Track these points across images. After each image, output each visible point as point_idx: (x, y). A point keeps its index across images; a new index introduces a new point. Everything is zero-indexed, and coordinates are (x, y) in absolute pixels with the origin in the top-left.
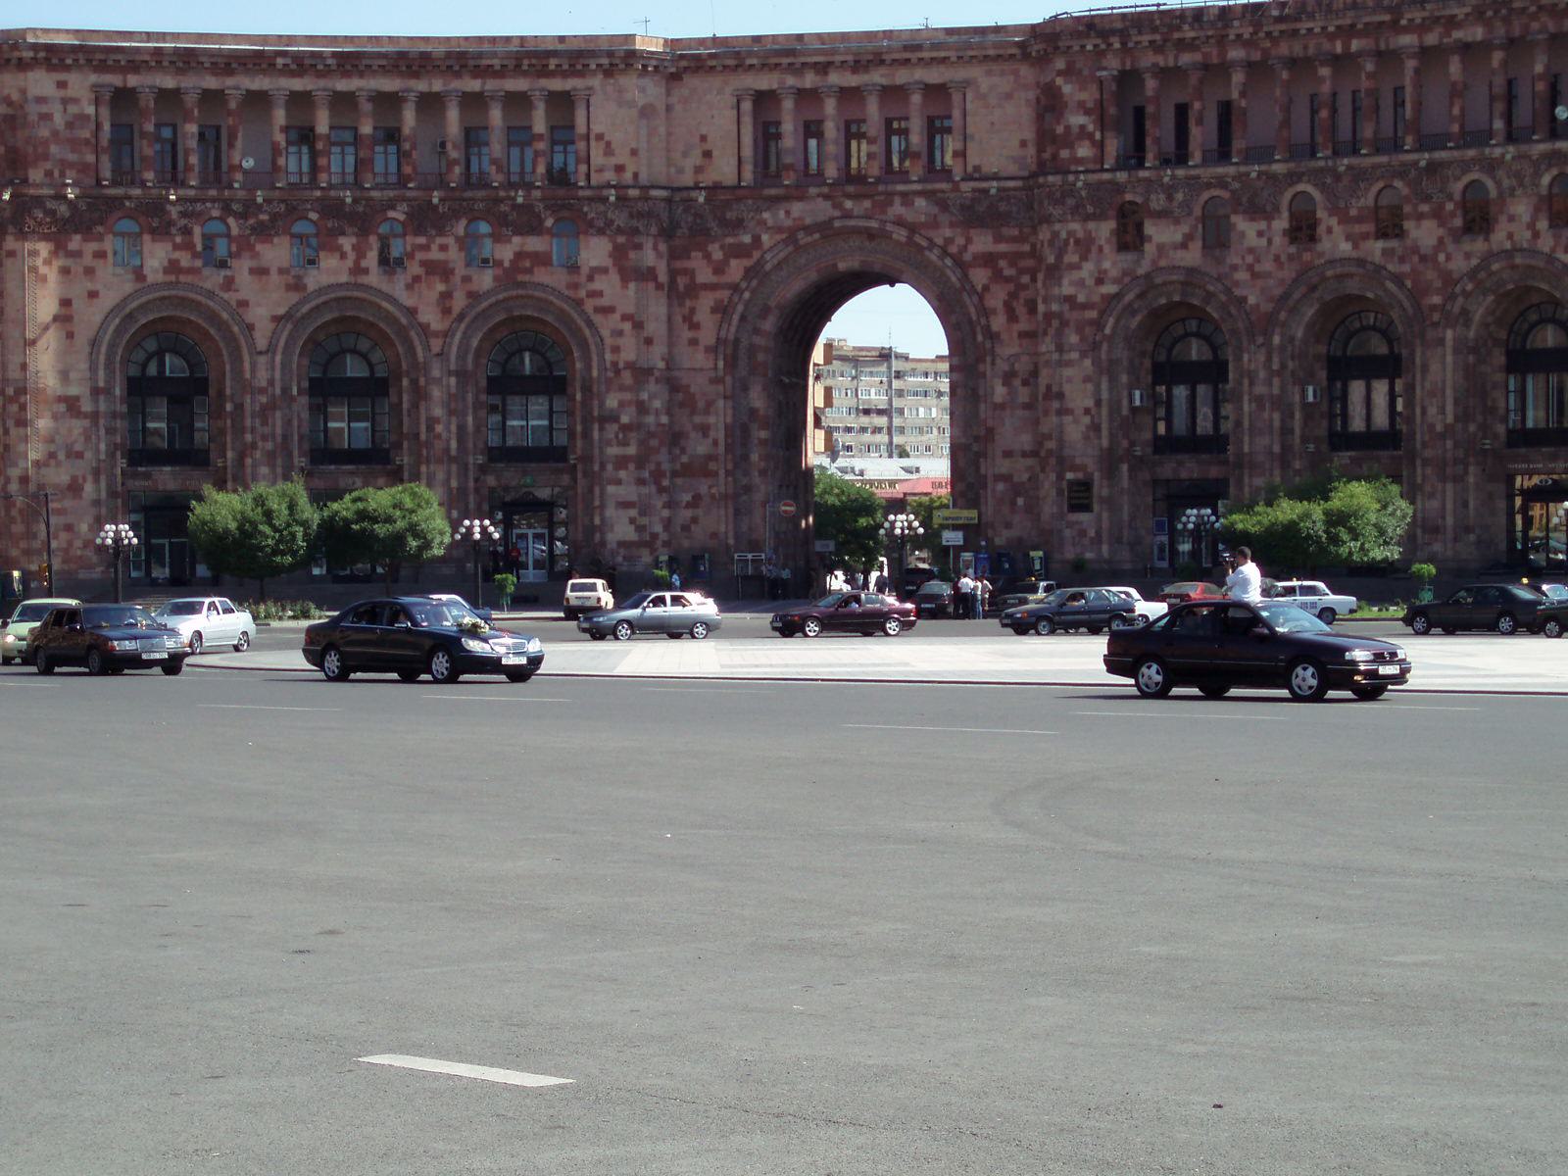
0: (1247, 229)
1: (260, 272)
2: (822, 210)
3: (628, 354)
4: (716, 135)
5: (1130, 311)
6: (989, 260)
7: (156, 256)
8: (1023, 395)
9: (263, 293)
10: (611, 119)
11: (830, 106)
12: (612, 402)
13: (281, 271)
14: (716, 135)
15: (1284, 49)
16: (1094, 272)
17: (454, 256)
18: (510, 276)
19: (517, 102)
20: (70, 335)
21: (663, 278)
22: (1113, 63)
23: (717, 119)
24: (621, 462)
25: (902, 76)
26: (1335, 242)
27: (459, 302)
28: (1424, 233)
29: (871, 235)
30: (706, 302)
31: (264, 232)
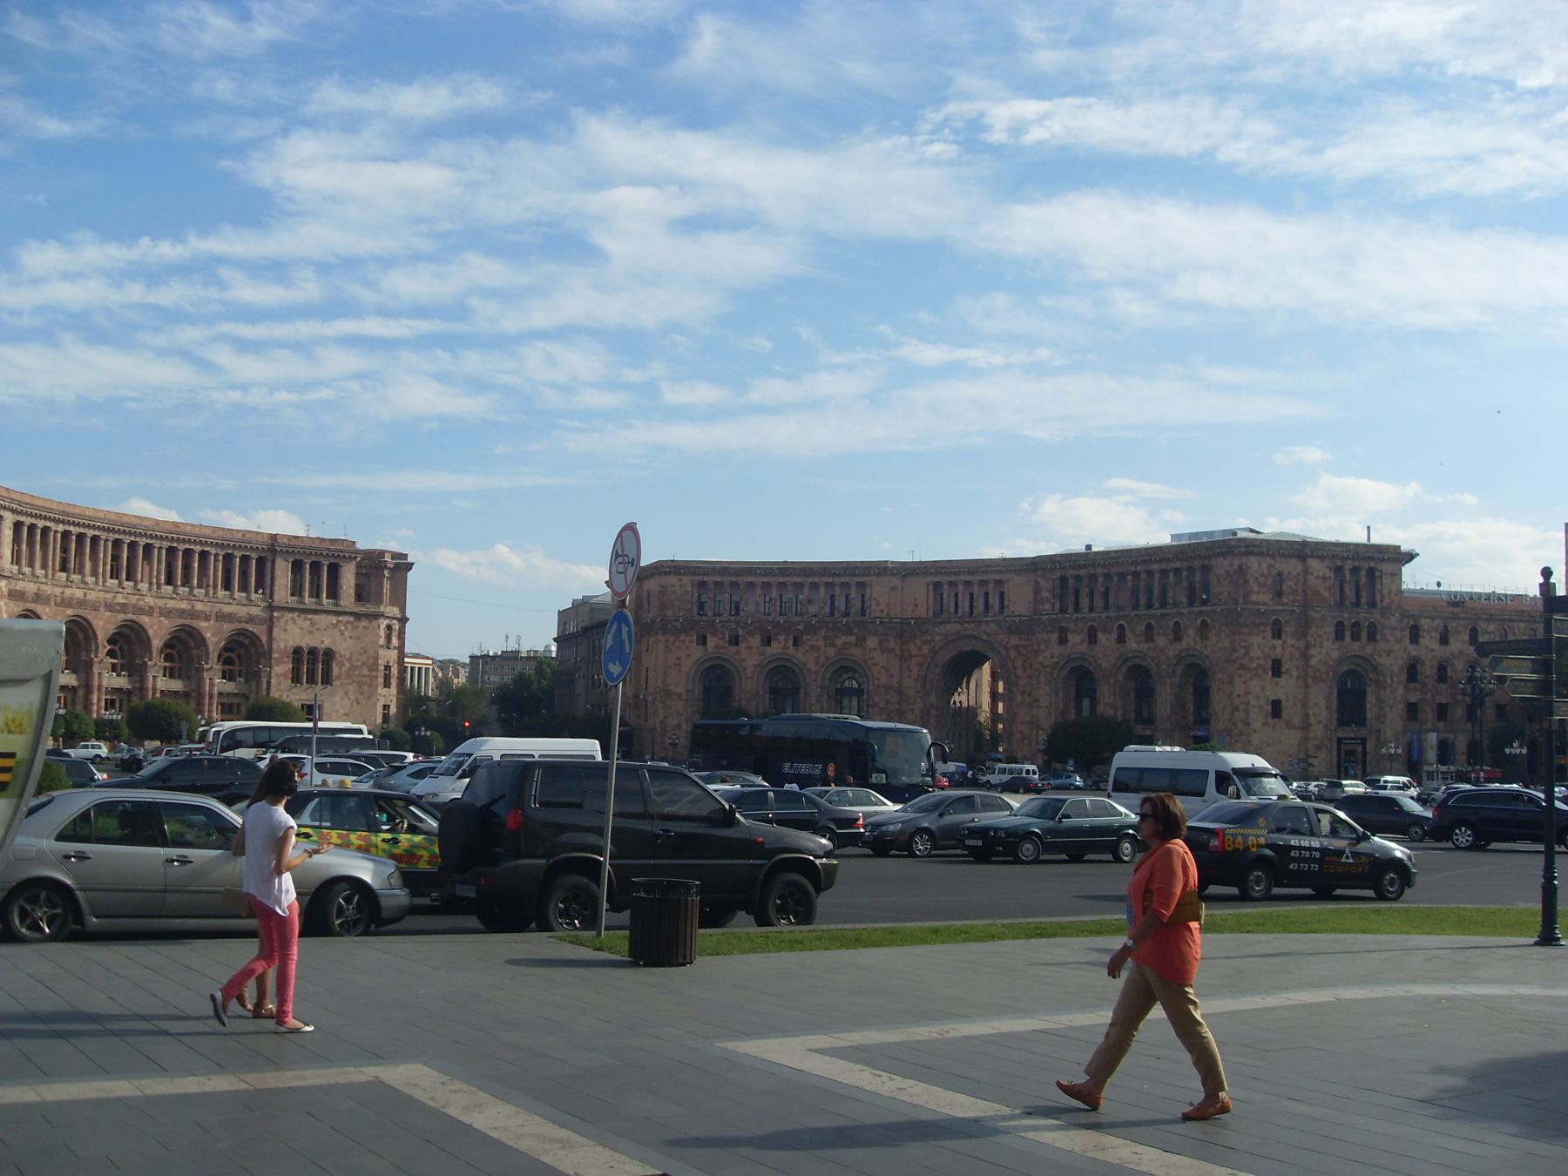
0: (1101, 636)
1: (750, 648)
3: (884, 680)
4: (919, 598)
6: (1016, 647)
8: (1028, 700)
9: (750, 658)
11: (961, 587)
12: (877, 699)
14: (919, 598)
15: (1115, 570)
16: (1051, 653)
17: (821, 643)
19: (845, 586)
22: (1058, 574)
23: (919, 590)
25: (985, 577)
26: (1132, 644)
27: (822, 660)
28: (1161, 641)
29: (975, 638)
30: (914, 662)
31: (751, 633)
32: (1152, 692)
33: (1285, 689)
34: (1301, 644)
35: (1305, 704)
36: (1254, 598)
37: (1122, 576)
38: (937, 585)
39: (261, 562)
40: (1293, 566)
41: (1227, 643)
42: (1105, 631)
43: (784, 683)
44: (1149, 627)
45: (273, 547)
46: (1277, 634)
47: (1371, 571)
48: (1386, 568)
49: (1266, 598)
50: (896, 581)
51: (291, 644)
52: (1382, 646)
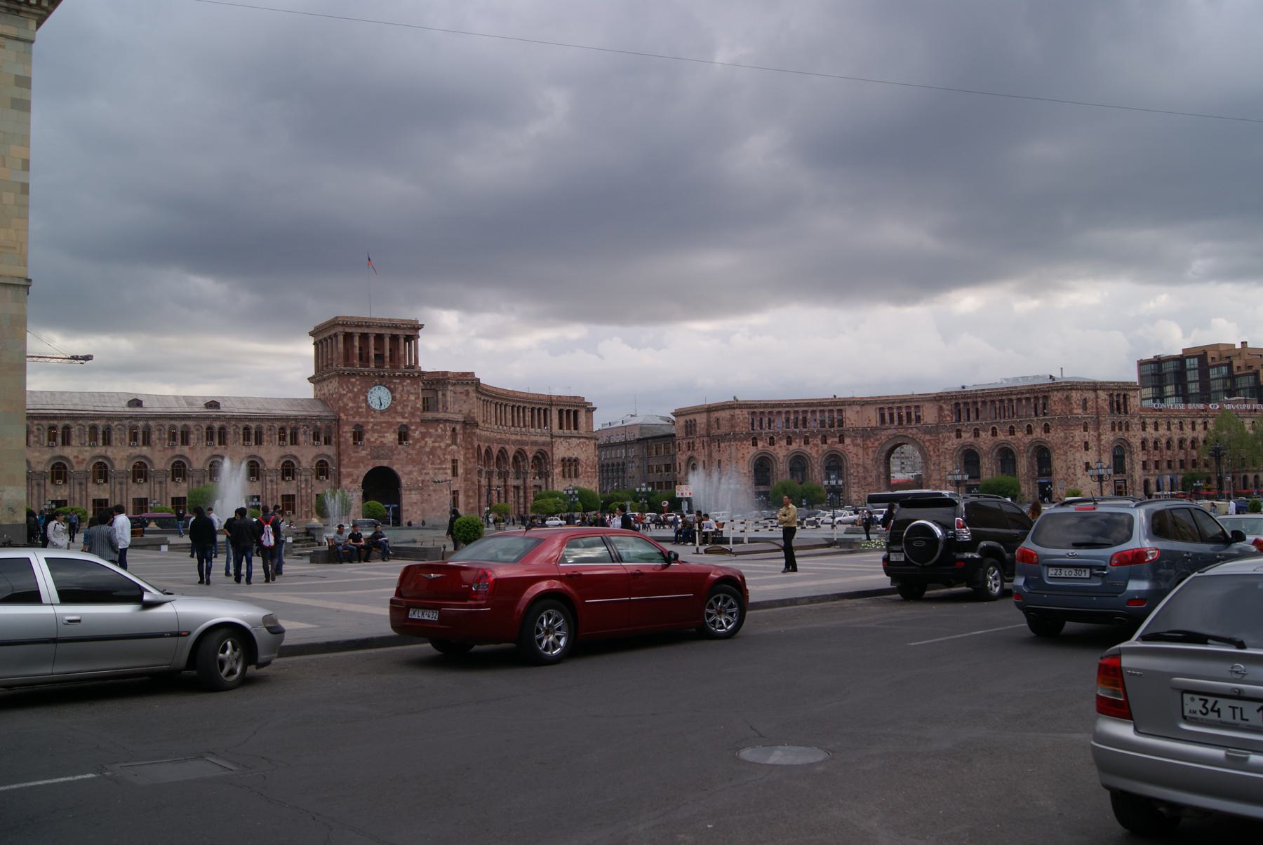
9: (781, 452)
16: (952, 443)
26: (1001, 436)
28: (1019, 434)
32: (1014, 461)
33: (1091, 456)
39: (545, 410)
41: (1062, 434)
42: (984, 431)
44: (1012, 427)
45: (551, 401)
46: (1086, 429)
47: (1125, 396)
49: (1080, 411)
50: (858, 408)
51: (561, 456)
52: (1131, 433)
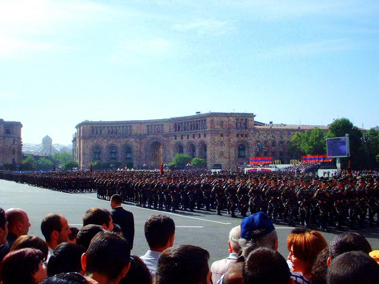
1: (104, 142)
2: (153, 136)
3: (136, 149)
4: (144, 130)
5: (176, 145)
6: (166, 140)
7: (95, 141)
10: (134, 128)
11: (153, 126)
12: (134, 153)
13: (106, 142)
16: (173, 142)
18: (126, 142)
20: (87, 148)
21: (139, 142)
22: (174, 122)
24: (135, 159)
28: (196, 138)
34: (228, 138)
35: (229, 153)
36: (216, 127)
37: (188, 122)
38: (148, 126)
40: (226, 119)
43: (112, 149)
48: (250, 119)
49: (219, 127)
50: (139, 125)
52: (249, 138)
